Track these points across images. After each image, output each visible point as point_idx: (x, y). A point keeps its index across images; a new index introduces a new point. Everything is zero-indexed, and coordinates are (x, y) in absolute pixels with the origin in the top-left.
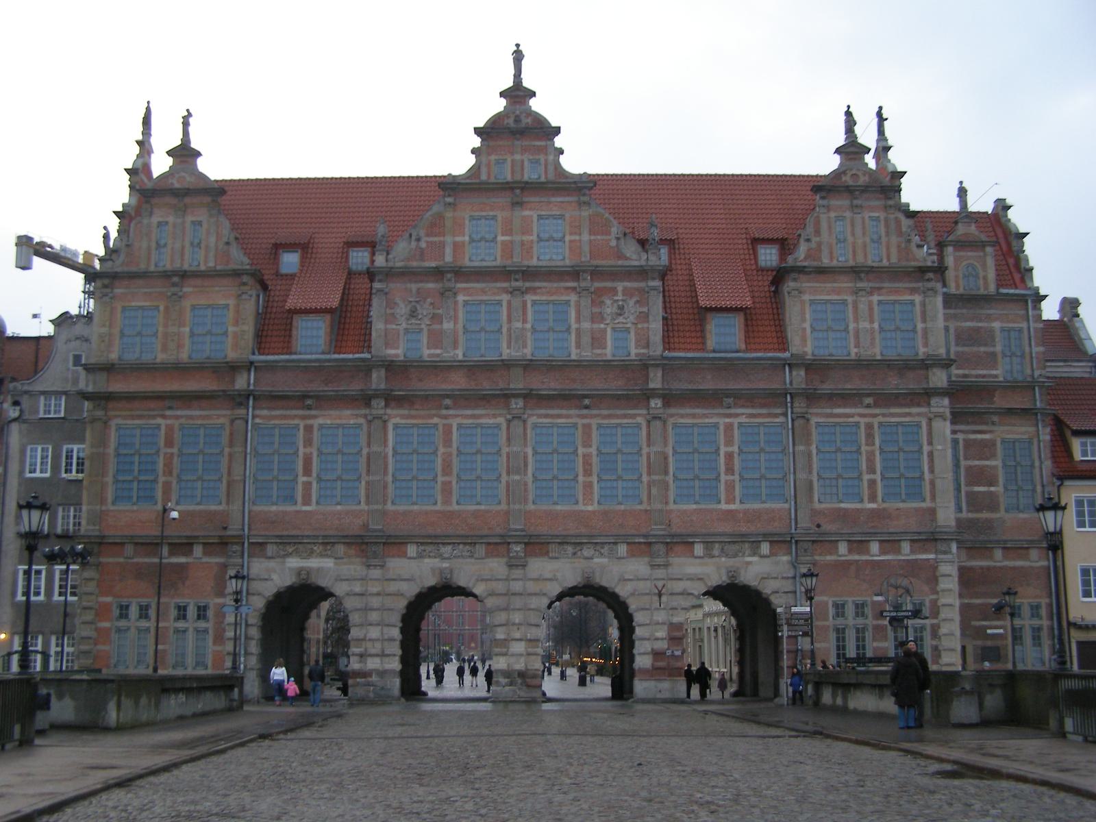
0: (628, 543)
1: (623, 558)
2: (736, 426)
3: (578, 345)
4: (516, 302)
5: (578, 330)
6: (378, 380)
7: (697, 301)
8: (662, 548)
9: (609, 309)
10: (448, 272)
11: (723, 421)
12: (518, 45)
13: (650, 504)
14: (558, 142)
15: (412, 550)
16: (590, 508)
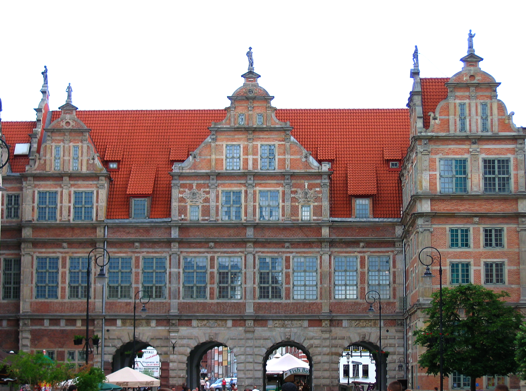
0: (309, 320)
1: (306, 328)
2: (366, 258)
3: (283, 215)
4: (250, 191)
5: (283, 207)
6: (175, 234)
7: (347, 190)
8: (327, 322)
9: (300, 195)
10: (212, 175)
11: (359, 255)
12: (250, 48)
13: (321, 299)
14: (274, 103)
15: (194, 323)
16: (288, 301)
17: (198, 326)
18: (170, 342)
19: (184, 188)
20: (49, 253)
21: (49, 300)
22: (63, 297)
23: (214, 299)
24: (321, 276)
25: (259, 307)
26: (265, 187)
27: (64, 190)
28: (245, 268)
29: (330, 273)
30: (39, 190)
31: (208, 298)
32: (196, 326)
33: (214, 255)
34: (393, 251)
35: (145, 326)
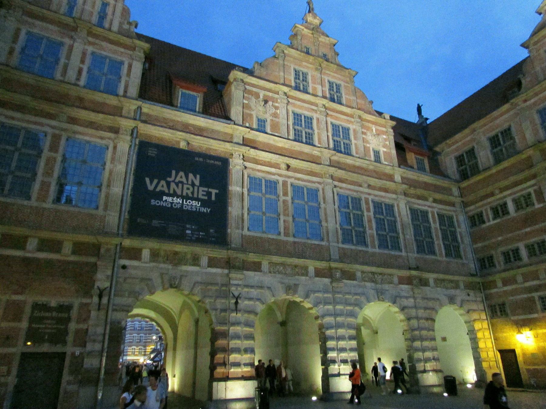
5: (356, 144)
16: (374, 250)
17: (270, 272)
18: (231, 295)
19: (249, 94)
20: (28, 122)
21: (9, 200)
22: (42, 198)
23: (289, 236)
24: (402, 225)
25: (345, 254)
26: (336, 120)
27: (76, 45)
28: (324, 203)
29: (409, 224)
30: (29, 29)
31: (282, 234)
32: (268, 271)
33: (286, 179)
34: (454, 211)
35: (190, 265)
